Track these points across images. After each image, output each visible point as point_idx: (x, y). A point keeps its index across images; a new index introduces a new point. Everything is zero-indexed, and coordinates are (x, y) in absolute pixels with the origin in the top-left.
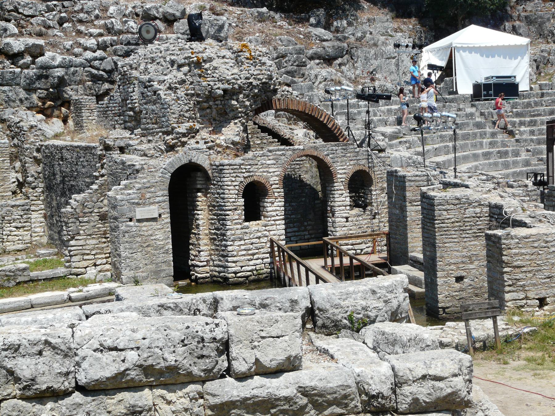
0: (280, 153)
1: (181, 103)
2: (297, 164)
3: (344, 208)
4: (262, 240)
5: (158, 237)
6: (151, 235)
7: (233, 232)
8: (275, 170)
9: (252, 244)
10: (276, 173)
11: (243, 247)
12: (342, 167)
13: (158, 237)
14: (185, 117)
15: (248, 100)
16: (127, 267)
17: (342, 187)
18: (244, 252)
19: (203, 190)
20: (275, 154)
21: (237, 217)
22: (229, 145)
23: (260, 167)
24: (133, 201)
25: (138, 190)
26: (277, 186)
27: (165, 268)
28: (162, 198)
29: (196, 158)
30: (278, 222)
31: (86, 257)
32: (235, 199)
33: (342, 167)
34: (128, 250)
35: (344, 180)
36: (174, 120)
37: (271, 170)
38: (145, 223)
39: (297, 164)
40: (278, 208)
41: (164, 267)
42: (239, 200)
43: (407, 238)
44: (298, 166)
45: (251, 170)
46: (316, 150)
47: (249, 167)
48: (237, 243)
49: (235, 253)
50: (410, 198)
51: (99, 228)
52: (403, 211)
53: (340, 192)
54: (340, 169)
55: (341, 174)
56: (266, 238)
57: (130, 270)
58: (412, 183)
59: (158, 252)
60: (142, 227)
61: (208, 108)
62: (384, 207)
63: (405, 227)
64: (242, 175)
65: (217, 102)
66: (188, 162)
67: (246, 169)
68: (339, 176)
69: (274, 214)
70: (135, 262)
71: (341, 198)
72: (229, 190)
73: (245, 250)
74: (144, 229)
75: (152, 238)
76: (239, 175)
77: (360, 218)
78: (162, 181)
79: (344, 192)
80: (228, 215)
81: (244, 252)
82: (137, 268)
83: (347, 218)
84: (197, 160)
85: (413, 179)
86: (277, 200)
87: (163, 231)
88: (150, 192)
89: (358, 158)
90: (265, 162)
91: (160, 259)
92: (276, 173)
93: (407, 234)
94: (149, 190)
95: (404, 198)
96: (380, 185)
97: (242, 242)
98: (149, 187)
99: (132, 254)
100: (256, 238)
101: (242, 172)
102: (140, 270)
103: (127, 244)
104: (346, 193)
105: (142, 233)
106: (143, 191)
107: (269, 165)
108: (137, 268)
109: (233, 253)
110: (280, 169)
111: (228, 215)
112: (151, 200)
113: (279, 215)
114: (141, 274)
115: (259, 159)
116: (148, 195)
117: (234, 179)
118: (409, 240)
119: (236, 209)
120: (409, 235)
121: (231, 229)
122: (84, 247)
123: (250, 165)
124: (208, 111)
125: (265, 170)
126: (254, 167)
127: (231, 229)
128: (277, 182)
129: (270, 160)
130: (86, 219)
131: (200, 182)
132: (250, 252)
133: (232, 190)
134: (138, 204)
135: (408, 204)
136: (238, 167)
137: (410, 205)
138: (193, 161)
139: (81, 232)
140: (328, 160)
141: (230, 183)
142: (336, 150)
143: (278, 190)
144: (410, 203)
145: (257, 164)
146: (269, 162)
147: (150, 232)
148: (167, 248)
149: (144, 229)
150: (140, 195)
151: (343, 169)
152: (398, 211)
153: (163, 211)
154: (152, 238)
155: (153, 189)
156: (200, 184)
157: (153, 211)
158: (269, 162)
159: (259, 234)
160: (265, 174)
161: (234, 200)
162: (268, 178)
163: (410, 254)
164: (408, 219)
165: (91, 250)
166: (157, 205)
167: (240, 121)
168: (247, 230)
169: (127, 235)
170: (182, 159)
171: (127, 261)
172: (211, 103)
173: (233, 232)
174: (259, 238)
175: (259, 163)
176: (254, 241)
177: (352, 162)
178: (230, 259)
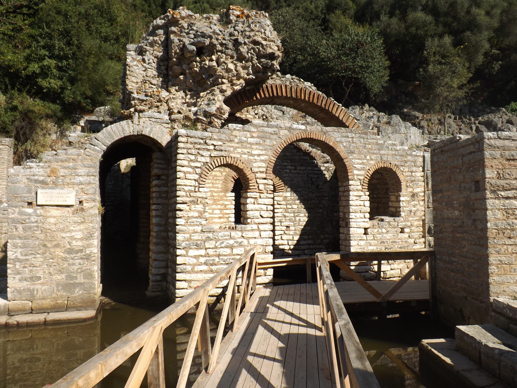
0: (270, 130)
1: (147, 66)
2: (315, 174)
3: (362, 215)
4: (235, 251)
5: (73, 234)
6: (62, 230)
7: (187, 236)
8: (261, 153)
9: (219, 256)
10: (263, 158)
11: (202, 260)
12: (360, 161)
13: (73, 234)
14: (152, 84)
15: (232, 62)
16: (16, 274)
17: (360, 187)
18: (204, 268)
19: (163, 177)
20: (263, 132)
21: (196, 214)
22: (201, 117)
23: (237, 145)
24: (36, 178)
25: (46, 162)
26: (264, 176)
27: (82, 281)
28: (86, 177)
29: (148, 129)
30: (261, 227)
32: (195, 187)
33: (360, 161)
34: (20, 250)
35: (362, 178)
36: (134, 85)
37: (254, 152)
38: (55, 212)
39: (315, 174)
40: (264, 207)
41: (80, 279)
42: (201, 189)
43: (486, 264)
44: (316, 176)
45: (223, 148)
46: (325, 133)
47: (221, 143)
48: (192, 252)
49: (189, 268)
50: (493, 182)
52: (474, 211)
53: (356, 193)
54: (358, 164)
55: (358, 170)
56: (243, 249)
57: (20, 280)
58: (497, 153)
59: (72, 256)
60: (46, 217)
62: (415, 219)
63: (482, 241)
66: (136, 133)
67: (215, 146)
68: (356, 172)
69: (257, 214)
70: (31, 268)
71: (359, 201)
72: (185, 173)
73: (205, 264)
74: (52, 220)
75: (64, 235)
76: (201, 152)
77: (384, 231)
78: (88, 154)
79: (362, 194)
80: (181, 210)
82: (34, 279)
83: (366, 229)
84: (150, 132)
85: (499, 143)
86: (262, 195)
87: (82, 227)
88: (65, 168)
89: (382, 152)
90: (245, 139)
91: (75, 268)
92: (263, 158)
93: (487, 256)
94: (66, 164)
95: (479, 186)
96: (410, 190)
97: (202, 252)
98: (66, 160)
99: (26, 255)
100: (226, 247)
101: (208, 150)
102: (39, 282)
103: (18, 241)
104: (366, 197)
105: (48, 227)
106: (54, 165)
107: (251, 144)
108: (34, 279)
109: (184, 267)
110: (270, 153)
111: (181, 210)
112: (67, 180)
113: (264, 216)
114: (40, 287)
115: (235, 133)
116: (62, 172)
117: (193, 157)
118: (492, 269)
119: (195, 203)
120: (492, 259)
121: (183, 232)
123: (220, 140)
124: (181, 77)
125: (246, 151)
126: (229, 144)
127: (183, 232)
128: (261, 170)
129: (252, 137)
131: (159, 165)
132: (214, 268)
133: (190, 173)
134: (44, 183)
135: (488, 194)
136: (202, 141)
137: (492, 196)
138: (143, 133)
140: (341, 149)
141: (185, 163)
142: (352, 138)
143: (265, 181)
144: (493, 192)
145: (231, 141)
146: (250, 140)
147: (61, 226)
148: (88, 252)
149: (52, 220)
150: (48, 170)
151: (360, 164)
153: (85, 197)
154: (64, 235)
155: (71, 164)
156: (158, 168)
157: (70, 197)
158: (250, 140)
159: (231, 242)
160: (245, 156)
161: (193, 189)
163: (492, 299)
164: (489, 225)
166: (77, 188)
167: (218, 88)
168: (210, 235)
169: (20, 227)
170: (126, 128)
171: (17, 267)
172: (184, 66)
173: (187, 236)
174: (232, 247)
175: (236, 140)
176: (222, 251)
177: (373, 157)
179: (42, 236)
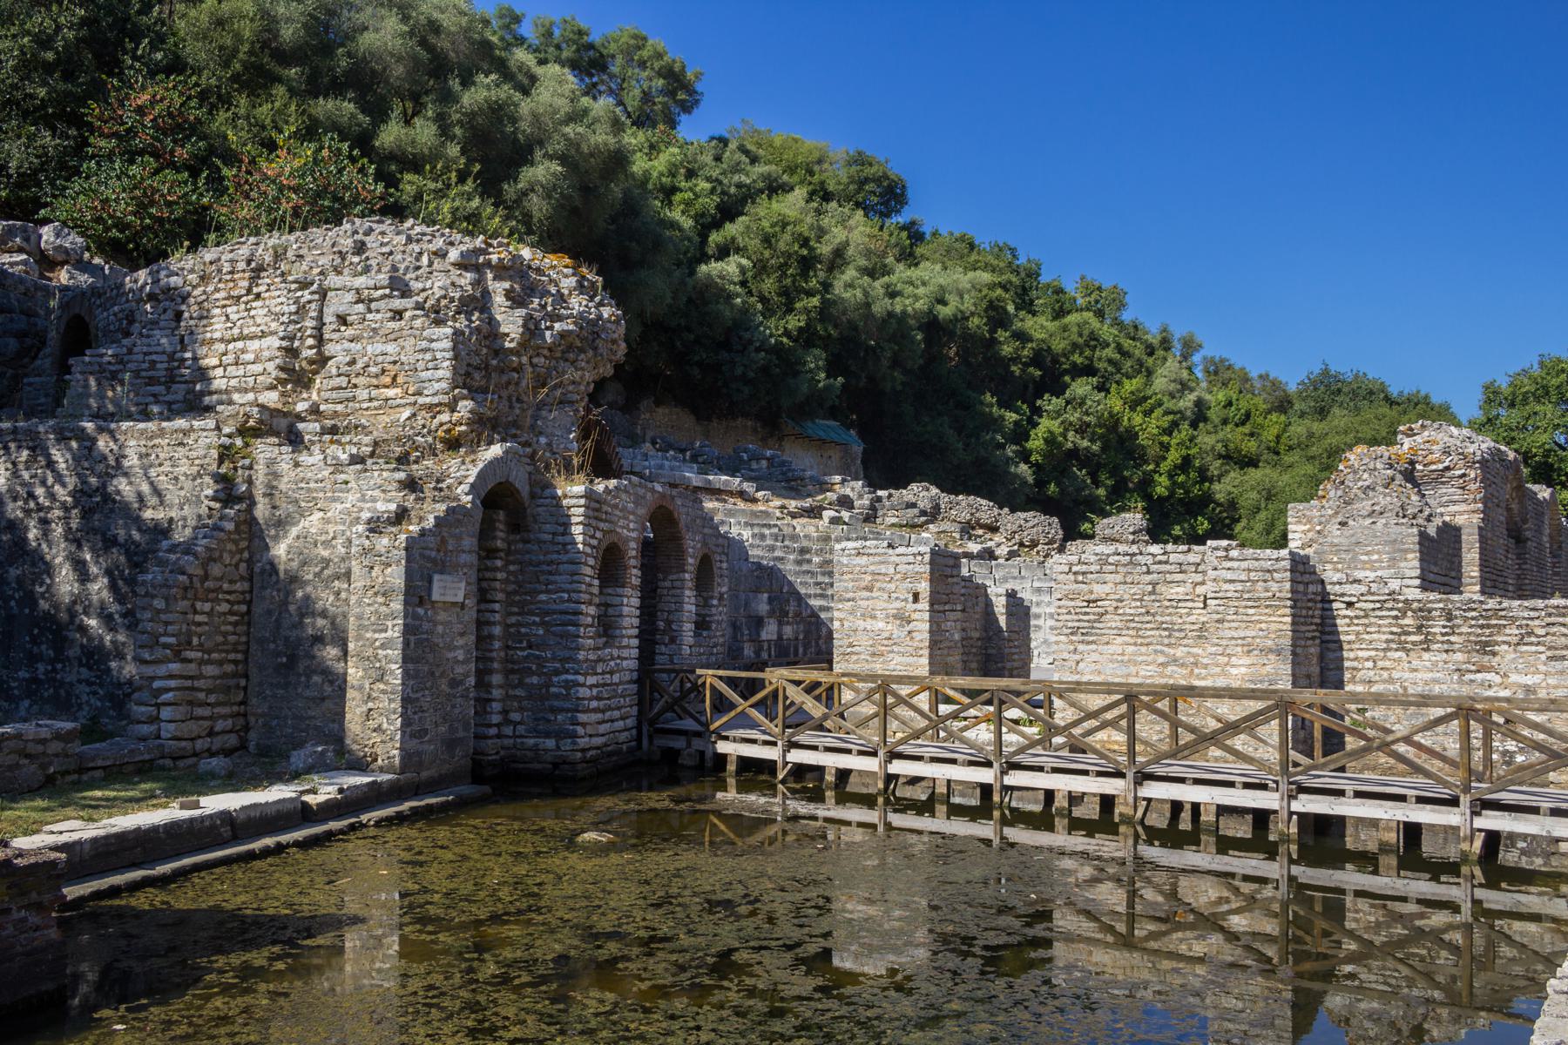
9: (604, 685)
18: (594, 704)
31: (199, 711)
51: (225, 634)
61: (514, 370)
64: (602, 525)
65: (535, 360)
81: (594, 704)
122: (196, 683)
130: (207, 607)
139: (195, 641)
152: (881, 625)
162: (627, 540)
165: (209, 692)
178: (583, 717)
179: (430, 657)
